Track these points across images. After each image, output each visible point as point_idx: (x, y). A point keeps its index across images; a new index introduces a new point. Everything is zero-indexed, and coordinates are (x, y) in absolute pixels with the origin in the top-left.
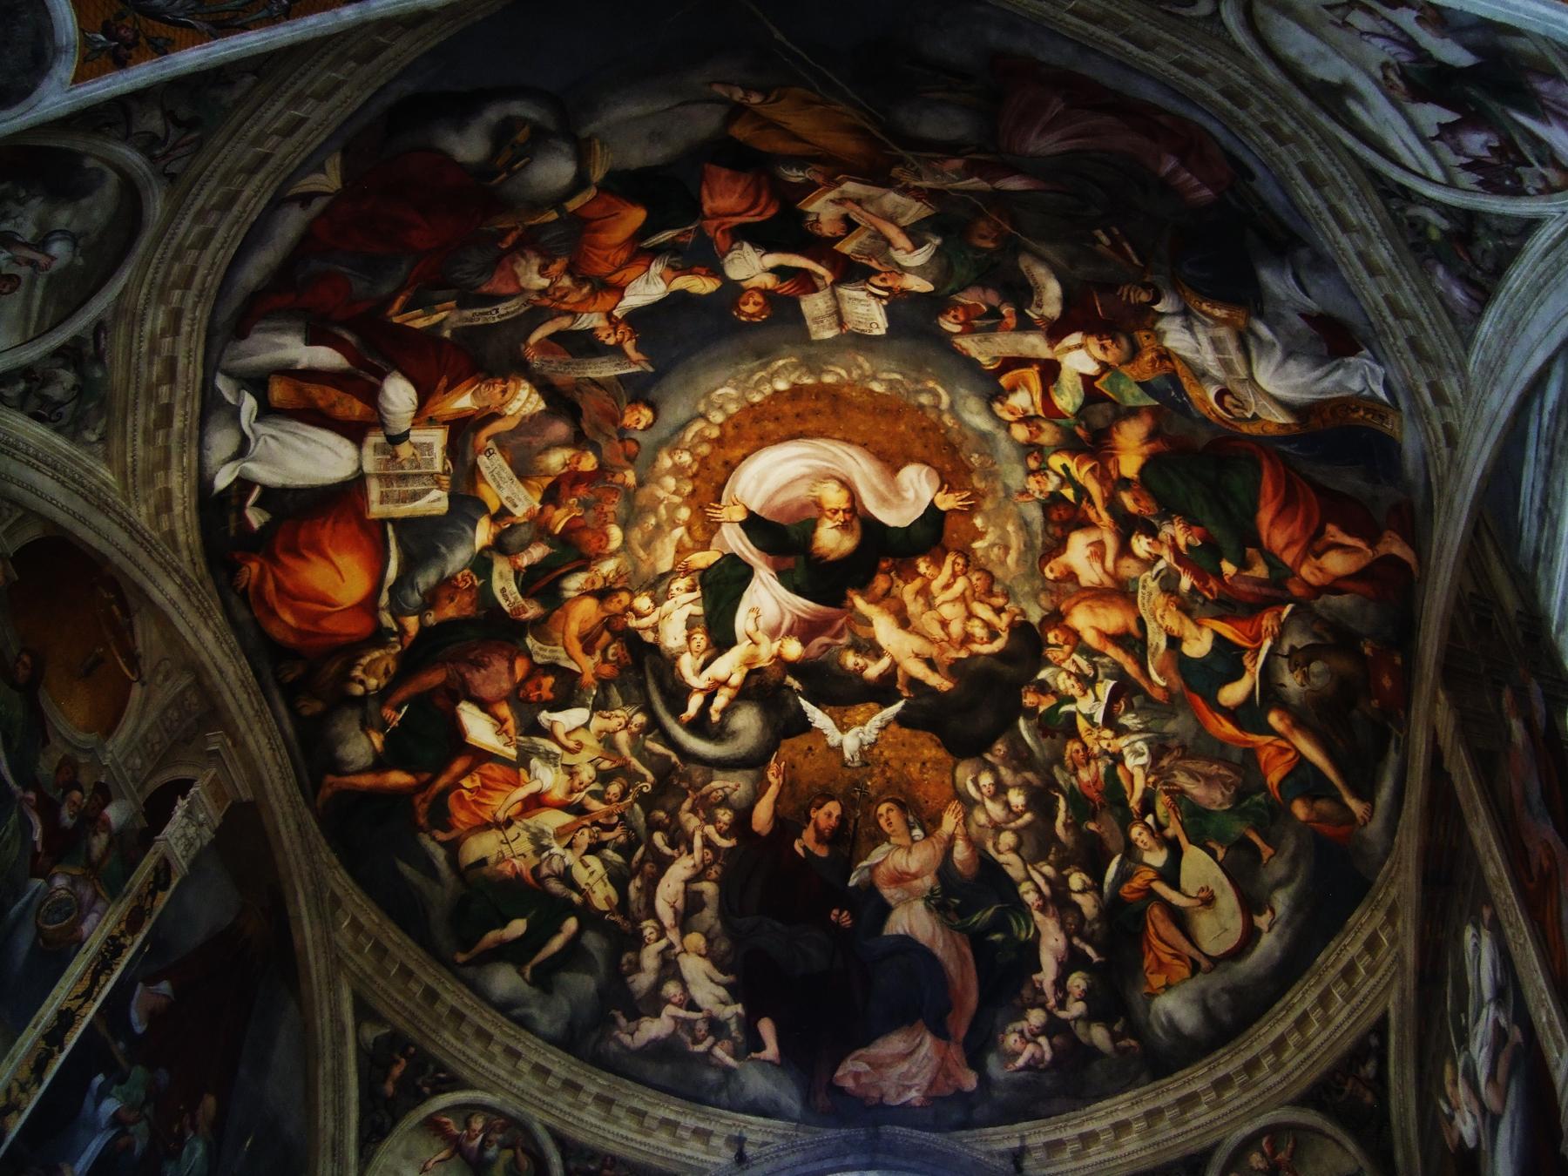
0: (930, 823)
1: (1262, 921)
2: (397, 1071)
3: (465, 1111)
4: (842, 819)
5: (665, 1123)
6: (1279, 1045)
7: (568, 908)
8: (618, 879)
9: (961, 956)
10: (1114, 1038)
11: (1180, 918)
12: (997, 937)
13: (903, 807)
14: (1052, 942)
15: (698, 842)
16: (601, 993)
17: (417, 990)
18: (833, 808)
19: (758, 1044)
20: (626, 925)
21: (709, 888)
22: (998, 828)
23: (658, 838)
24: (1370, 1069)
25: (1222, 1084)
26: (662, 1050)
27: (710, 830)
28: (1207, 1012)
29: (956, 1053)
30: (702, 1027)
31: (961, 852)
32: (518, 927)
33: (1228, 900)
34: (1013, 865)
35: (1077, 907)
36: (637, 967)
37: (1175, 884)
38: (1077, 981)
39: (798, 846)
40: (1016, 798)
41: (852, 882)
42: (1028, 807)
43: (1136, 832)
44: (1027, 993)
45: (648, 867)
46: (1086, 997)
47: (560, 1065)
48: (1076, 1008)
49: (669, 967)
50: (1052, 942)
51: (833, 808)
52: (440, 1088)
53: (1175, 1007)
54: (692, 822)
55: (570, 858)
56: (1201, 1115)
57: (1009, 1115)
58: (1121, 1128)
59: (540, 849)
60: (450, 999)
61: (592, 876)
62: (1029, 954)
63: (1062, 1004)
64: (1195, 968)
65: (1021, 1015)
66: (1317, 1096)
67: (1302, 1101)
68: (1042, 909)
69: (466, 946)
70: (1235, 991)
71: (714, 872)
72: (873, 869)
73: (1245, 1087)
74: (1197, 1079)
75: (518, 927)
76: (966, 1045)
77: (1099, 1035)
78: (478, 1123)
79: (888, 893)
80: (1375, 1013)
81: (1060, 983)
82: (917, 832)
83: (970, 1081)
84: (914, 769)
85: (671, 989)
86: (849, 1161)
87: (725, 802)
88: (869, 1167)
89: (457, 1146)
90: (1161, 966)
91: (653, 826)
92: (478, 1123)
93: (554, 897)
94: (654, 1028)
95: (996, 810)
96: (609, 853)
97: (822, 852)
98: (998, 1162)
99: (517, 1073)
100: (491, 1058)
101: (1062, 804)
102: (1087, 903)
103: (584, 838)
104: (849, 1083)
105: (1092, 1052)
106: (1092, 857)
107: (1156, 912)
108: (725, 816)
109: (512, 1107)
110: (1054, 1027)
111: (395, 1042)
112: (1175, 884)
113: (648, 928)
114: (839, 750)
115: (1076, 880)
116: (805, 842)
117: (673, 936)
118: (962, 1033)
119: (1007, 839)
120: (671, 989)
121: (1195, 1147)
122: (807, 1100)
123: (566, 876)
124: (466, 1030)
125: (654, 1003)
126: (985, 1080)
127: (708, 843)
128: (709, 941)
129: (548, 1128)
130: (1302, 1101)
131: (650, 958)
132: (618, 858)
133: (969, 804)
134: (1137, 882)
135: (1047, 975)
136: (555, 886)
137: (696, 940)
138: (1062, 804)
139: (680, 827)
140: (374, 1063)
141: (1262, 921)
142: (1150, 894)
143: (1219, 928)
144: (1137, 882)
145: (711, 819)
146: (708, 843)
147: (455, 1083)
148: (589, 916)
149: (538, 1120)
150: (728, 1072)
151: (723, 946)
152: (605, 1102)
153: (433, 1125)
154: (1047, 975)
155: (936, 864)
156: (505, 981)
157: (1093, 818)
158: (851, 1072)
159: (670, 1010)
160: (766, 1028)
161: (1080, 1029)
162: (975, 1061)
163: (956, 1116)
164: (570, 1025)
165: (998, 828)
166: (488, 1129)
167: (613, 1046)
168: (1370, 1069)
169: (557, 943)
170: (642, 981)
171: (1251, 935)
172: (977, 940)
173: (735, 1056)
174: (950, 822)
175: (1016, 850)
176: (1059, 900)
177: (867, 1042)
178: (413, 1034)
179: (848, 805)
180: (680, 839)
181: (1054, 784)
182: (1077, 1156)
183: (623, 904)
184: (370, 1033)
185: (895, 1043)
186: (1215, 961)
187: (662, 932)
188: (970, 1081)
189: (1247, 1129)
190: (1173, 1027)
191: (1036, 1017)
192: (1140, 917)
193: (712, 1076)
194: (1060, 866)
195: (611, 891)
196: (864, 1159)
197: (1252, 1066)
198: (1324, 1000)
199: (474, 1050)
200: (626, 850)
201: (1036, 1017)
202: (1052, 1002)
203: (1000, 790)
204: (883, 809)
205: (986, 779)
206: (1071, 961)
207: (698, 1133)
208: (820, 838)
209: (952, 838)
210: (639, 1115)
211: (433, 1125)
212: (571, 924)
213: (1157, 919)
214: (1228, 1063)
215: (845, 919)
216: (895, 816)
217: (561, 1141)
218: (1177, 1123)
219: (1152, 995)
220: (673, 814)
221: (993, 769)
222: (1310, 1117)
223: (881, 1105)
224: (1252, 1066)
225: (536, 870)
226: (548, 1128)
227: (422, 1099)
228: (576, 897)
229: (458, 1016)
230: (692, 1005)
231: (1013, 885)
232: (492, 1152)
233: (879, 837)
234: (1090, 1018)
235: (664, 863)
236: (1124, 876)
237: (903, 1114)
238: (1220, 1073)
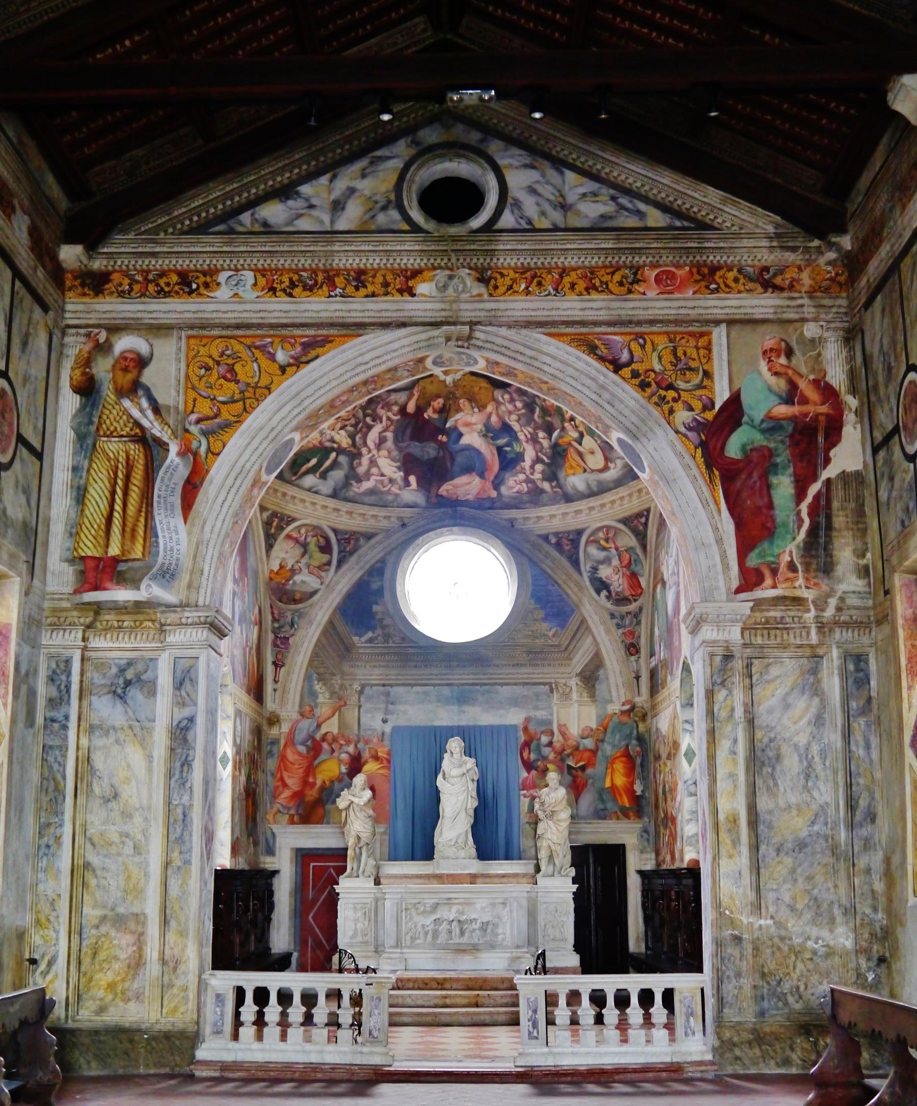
0: (482, 408)
1: (611, 465)
2: (275, 524)
3: (299, 527)
4: (444, 405)
5: (373, 516)
6: (613, 502)
7: (333, 449)
8: (352, 436)
9: (493, 454)
10: (552, 487)
11: (580, 454)
12: (508, 449)
13: (470, 400)
14: (530, 453)
15: (384, 419)
16: (347, 477)
17: (279, 494)
18: (441, 401)
19: (407, 484)
20: (355, 451)
21: (389, 435)
22: (510, 413)
23: (368, 420)
24: (643, 520)
25: (591, 509)
26: (372, 492)
27: (390, 414)
28: (588, 485)
29: (488, 485)
30: (386, 481)
31: (494, 419)
32: (314, 461)
33: (599, 456)
34: (516, 427)
35: (541, 444)
36: (360, 464)
37: (580, 444)
38: (539, 467)
39: (426, 416)
40: (519, 405)
41: (448, 425)
42: (523, 407)
43: (566, 425)
44: (518, 468)
45: (364, 430)
46: (543, 472)
47: (332, 503)
48: (537, 476)
49: (373, 462)
50: (530, 453)
51: (441, 401)
52: (288, 524)
53: (576, 481)
54: (381, 412)
55: (333, 433)
56: (583, 517)
57: (508, 507)
58: (552, 516)
59: (322, 433)
60: (290, 493)
61: (343, 439)
62: (520, 457)
63: (532, 474)
64: (585, 471)
65: (516, 474)
66: (625, 521)
67: (620, 521)
68: (527, 442)
69: (295, 474)
70: (600, 483)
71: (392, 428)
72: (456, 421)
73: (599, 511)
74: (583, 505)
75: (314, 461)
76: (493, 482)
77: (546, 486)
78: (303, 531)
79: (462, 429)
80: (647, 506)
81: (532, 467)
82: (476, 410)
83: (494, 494)
84: (476, 389)
85: (374, 470)
86: (446, 522)
87: (396, 403)
88: (454, 525)
89: (296, 541)
90: (572, 467)
91: (365, 416)
92: (303, 531)
93: (326, 448)
94: (367, 485)
95: (510, 407)
96: (349, 428)
97: (436, 416)
98: (504, 523)
99: (316, 510)
100: (306, 507)
101: (538, 409)
102: (546, 443)
103: (339, 425)
104: (444, 493)
105: (542, 491)
106: (549, 430)
107: (572, 450)
108: (396, 408)
109: (315, 522)
110: (528, 481)
111: (274, 514)
112: (580, 444)
113: (364, 450)
114: (444, 381)
115: (541, 434)
116: (429, 414)
117: (374, 452)
118: (492, 478)
119: (514, 417)
120: (374, 470)
121: (579, 527)
122: (428, 499)
123: (332, 440)
124: (297, 501)
125: (368, 475)
126: (499, 494)
127: (389, 419)
128: (389, 452)
129: (329, 527)
130: (620, 521)
131: (365, 461)
132: (352, 429)
133: (498, 403)
134: (565, 440)
135: (527, 464)
136: (328, 444)
137: (384, 453)
138: (538, 409)
139: (377, 414)
140: (267, 524)
141: (611, 465)
142: (570, 444)
143: (596, 461)
144: (565, 440)
145: (389, 410)
146: (389, 419)
147: (294, 520)
148: (340, 451)
149: (324, 525)
150: (397, 495)
151: (395, 453)
152: (350, 513)
153: (289, 537)
154: (527, 464)
155: (484, 421)
156: (309, 480)
157: (550, 416)
158: (445, 489)
159: (373, 478)
160: (412, 479)
161: (539, 483)
162: (496, 487)
163: (488, 504)
164: (335, 490)
165: (510, 413)
166: (307, 532)
167: (351, 493)
168: (643, 520)
169: (328, 463)
170: (361, 470)
171: (605, 469)
172: (500, 449)
173: (400, 489)
174: (490, 408)
175: (518, 421)
176: (534, 440)
177: (452, 478)
178: (279, 510)
179: (447, 399)
180: (376, 418)
181: (535, 402)
182: (535, 523)
183: (354, 444)
184: (266, 515)
185: (463, 480)
186: (593, 471)
187: (370, 451)
188: (494, 494)
189: (599, 525)
190: (574, 488)
191: (522, 477)
192: (565, 450)
193: (390, 498)
194: (535, 429)
195: (350, 441)
196: (452, 522)
197: (603, 505)
198: (630, 495)
199: (300, 507)
200: (355, 426)
201: (522, 477)
202: (528, 472)
203: (512, 400)
204: (461, 401)
205: (507, 397)
206: (538, 460)
207: (385, 517)
208: (435, 411)
209: (491, 414)
210: (363, 515)
211: (289, 537)
212: (333, 455)
213: (572, 453)
214: (594, 502)
215: (444, 439)
216: (467, 403)
217: (335, 531)
218: (573, 518)
219: (567, 476)
220: (374, 411)
221: (510, 393)
222: (621, 526)
223: (457, 500)
224: (603, 505)
225: (320, 443)
226: (329, 527)
227: (282, 529)
228: (335, 446)
229: (293, 497)
230: (382, 475)
231: (516, 433)
232: (309, 540)
233: (459, 410)
234: (544, 479)
235: (369, 428)
236: (560, 437)
237: (466, 503)
238: (591, 505)
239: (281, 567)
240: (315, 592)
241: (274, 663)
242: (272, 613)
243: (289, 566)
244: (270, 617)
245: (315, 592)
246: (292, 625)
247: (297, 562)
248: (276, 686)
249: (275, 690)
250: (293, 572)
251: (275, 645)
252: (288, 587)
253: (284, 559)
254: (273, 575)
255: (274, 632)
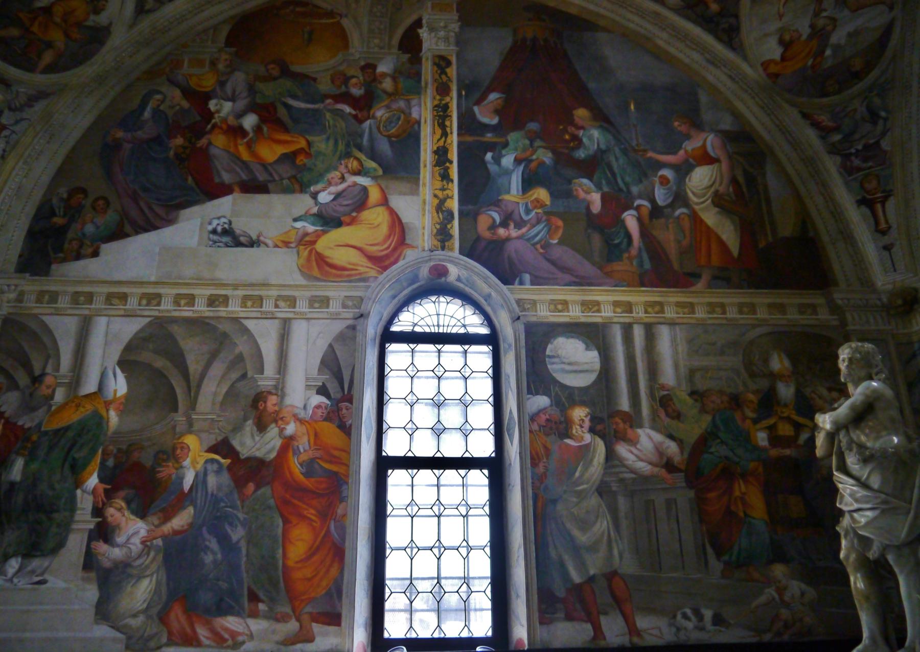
239: (786, 45)
240: (888, 31)
241: (862, 202)
242: (816, 125)
243: (806, 31)
244: (811, 135)
245: (888, 31)
246: (873, 116)
247: (816, 14)
248: (886, 240)
249: (887, 248)
250: (820, 35)
251: (848, 170)
252: (829, 63)
253: (781, 31)
254: (773, 69)
255: (833, 150)
